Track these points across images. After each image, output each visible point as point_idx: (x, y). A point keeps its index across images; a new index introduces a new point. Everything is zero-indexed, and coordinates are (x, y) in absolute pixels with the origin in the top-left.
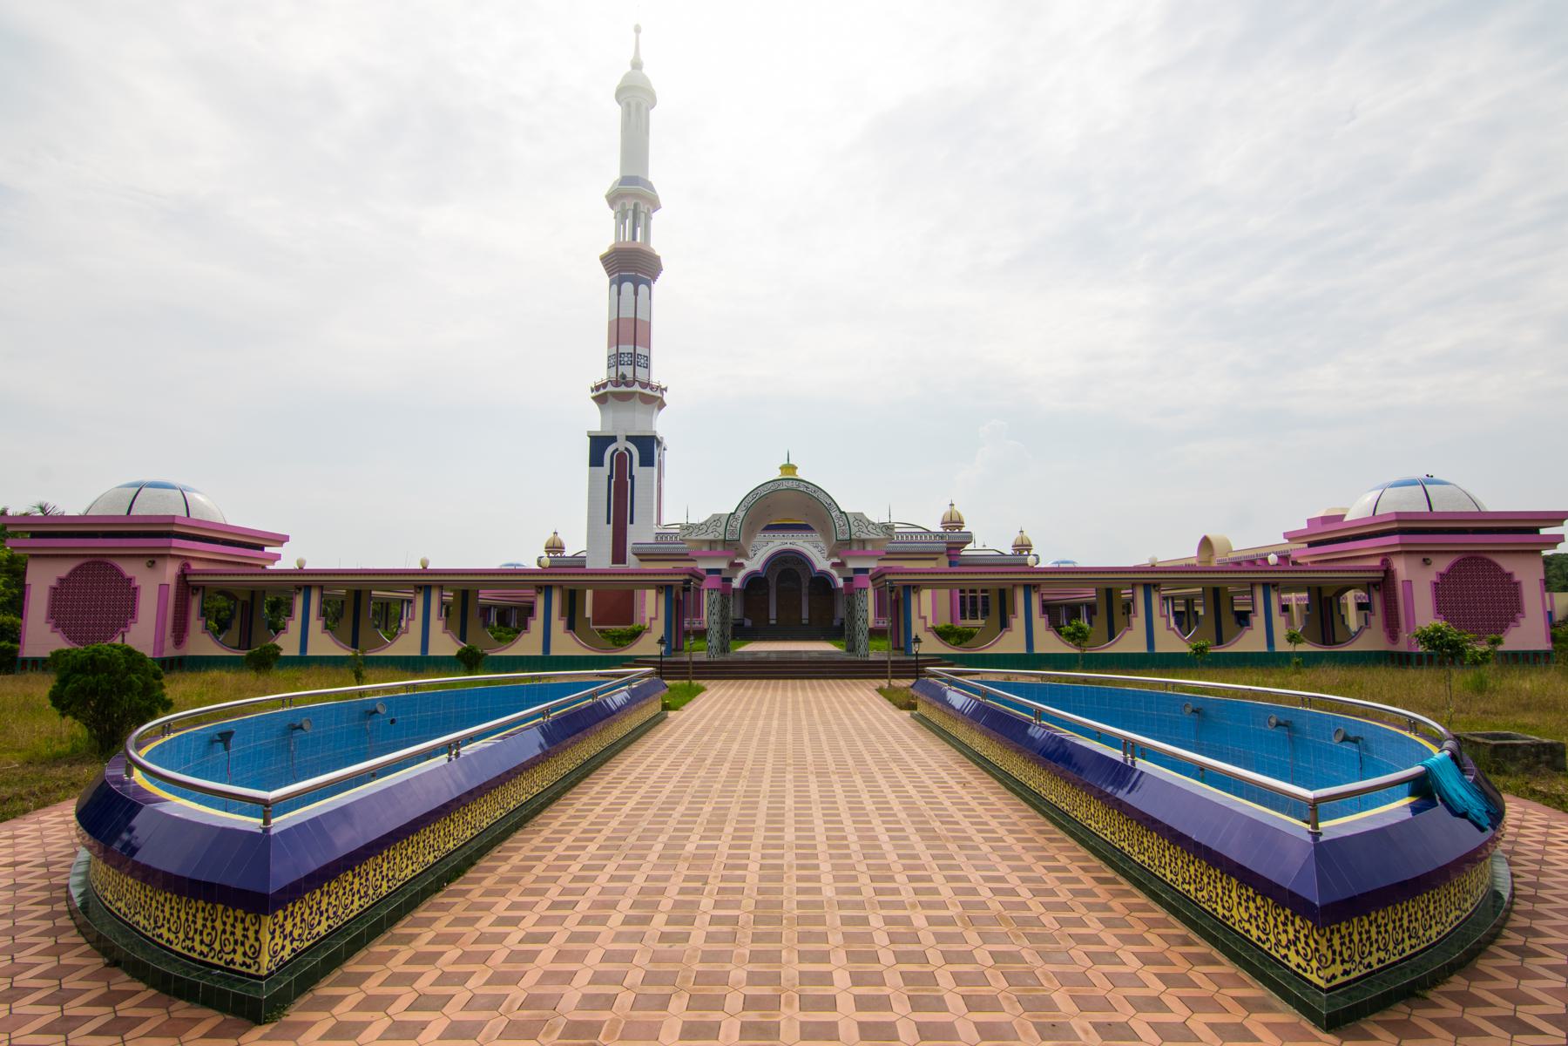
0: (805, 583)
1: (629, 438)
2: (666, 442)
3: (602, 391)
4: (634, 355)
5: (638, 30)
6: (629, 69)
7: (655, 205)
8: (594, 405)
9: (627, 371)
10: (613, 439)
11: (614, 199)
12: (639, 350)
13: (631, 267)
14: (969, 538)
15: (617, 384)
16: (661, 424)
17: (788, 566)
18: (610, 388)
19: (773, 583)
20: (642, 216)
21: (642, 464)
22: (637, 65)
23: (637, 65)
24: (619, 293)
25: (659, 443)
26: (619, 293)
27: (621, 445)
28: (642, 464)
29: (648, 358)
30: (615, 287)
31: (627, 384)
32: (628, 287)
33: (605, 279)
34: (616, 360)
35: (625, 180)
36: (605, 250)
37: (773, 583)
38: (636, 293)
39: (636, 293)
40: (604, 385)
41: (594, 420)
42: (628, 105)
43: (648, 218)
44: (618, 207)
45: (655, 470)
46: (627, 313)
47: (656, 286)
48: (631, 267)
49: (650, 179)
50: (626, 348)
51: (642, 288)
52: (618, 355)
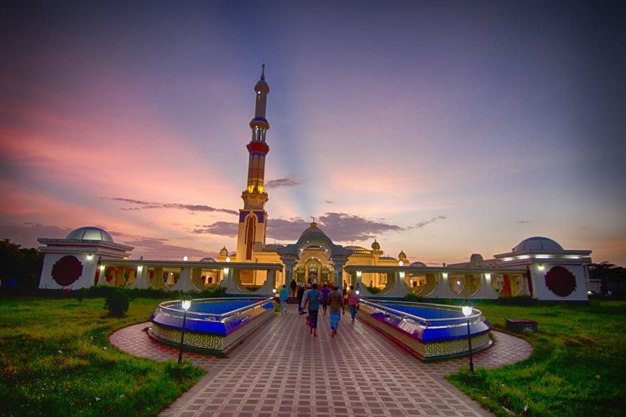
1: (254, 212)
2: (268, 214)
5: (263, 66)
6: (259, 79)
11: (252, 125)
13: (258, 149)
14: (382, 253)
21: (259, 222)
22: (263, 78)
23: (263, 78)
24: (253, 159)
26: (253, 159)
27: (252, 214)
28: (259, 222)
32: (256, 156)
33: (248, 153)
34: (250, 183)
35: (256, 119)
36: (249, 143)
38: (259, 159)
45: (263, 225)
46: (255, 166)
47: (267, 156)
48: (258, 149)
49: (266, 118)
51: (262, 157)
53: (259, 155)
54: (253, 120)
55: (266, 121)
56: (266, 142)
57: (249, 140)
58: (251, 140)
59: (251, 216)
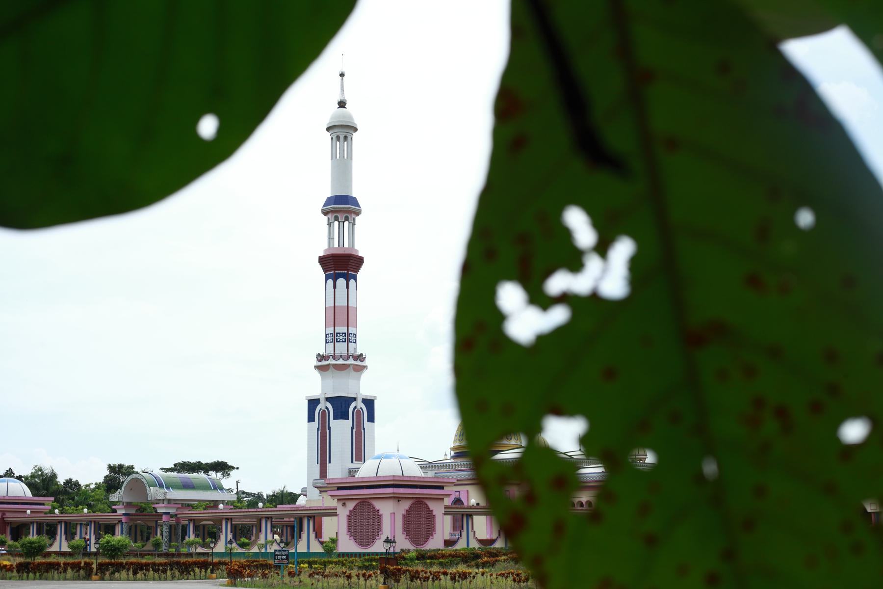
3: (324, 363)
4: (347, 334)
8: (317, 374)
12: (351, 330)
13: (341, 265)
18: (331, 361)
24: (335, 287)
26: (335, 287)
30: (330, 282)
32: (341, 282)
33: (324, 275)
34: (333, 338)
36: (322, 254)
38: (348, 287)
39: (348, 287)
41: (316, 386)
43: (354, 224)
46: (341, 302)
47: (360, 275)
48: (341, 265)
50: (341, 329)
51: (352, 282)
52: (335, 334)
53: (347, 278)
54: (329, 201)
55: (354, 201)
56: (356, 247)
57: (322, 249)
58: (326, 247)
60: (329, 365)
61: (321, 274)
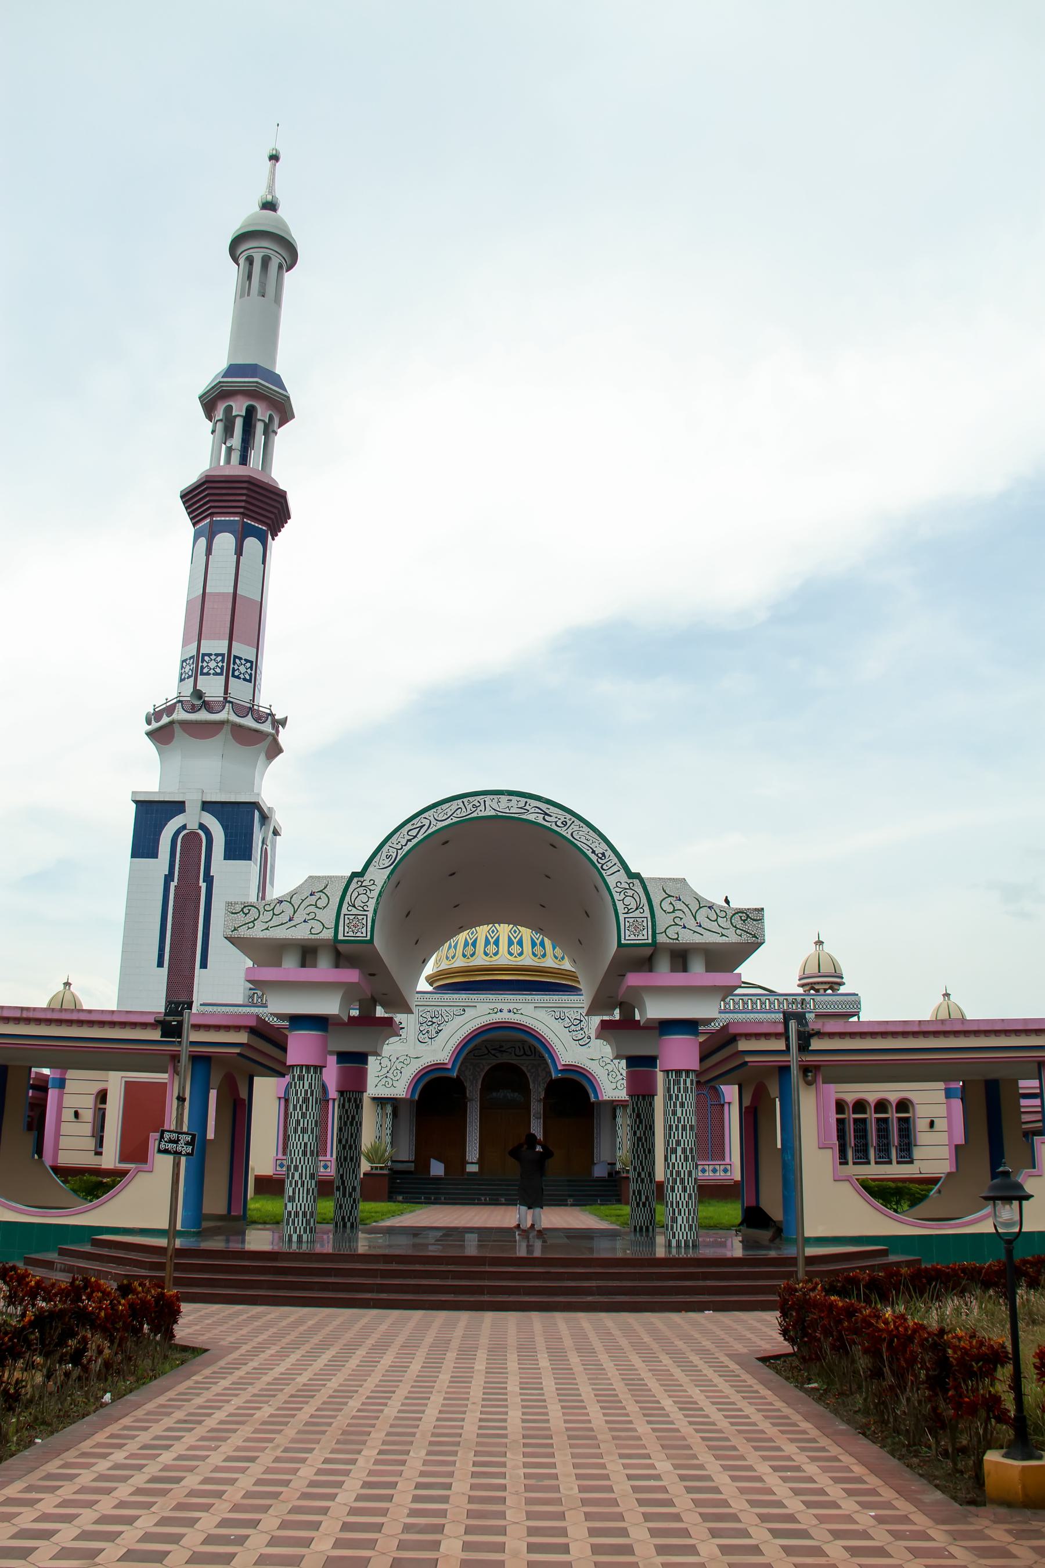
0: (537, 1093)
2: (279, 818)
3: (165, 720)
7: (283, 411)
9: (212, 687)
10: (178, 807)
15: (194, 709)
16: (274, 786)
17: (504, 1062)
18: (180, 715)
19: (474, 1092)
20: (260, 428)
25: (264, 818)
29: (253, 665)
31: (207, 706)
32: (225, 541)
37: (474, 1092)
40: (170, 710)
42: (250, 260)
44: (219, 414)
52: (199, 657)
59: (193, 826)
60: (172, 723)
61: (185, 527)
